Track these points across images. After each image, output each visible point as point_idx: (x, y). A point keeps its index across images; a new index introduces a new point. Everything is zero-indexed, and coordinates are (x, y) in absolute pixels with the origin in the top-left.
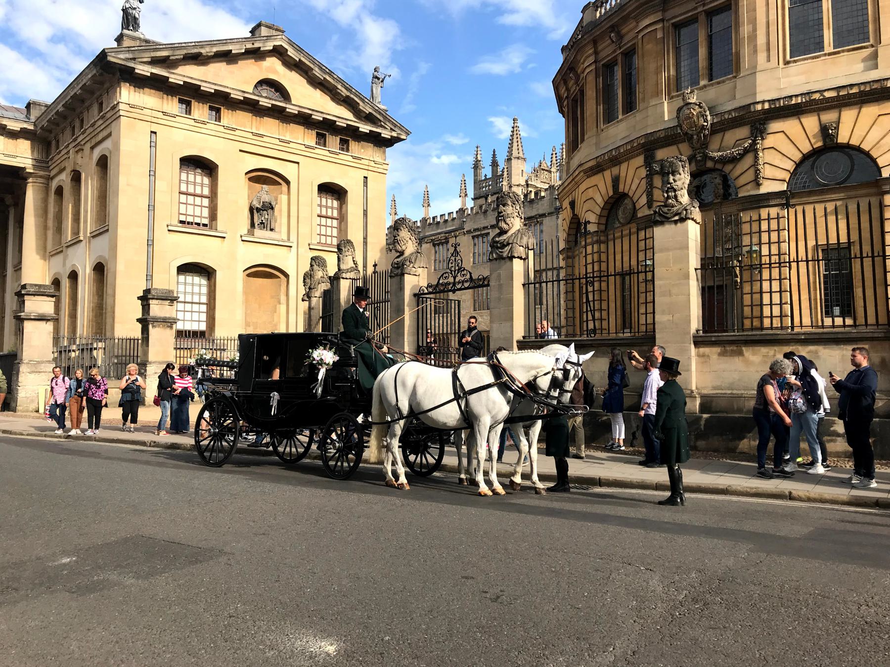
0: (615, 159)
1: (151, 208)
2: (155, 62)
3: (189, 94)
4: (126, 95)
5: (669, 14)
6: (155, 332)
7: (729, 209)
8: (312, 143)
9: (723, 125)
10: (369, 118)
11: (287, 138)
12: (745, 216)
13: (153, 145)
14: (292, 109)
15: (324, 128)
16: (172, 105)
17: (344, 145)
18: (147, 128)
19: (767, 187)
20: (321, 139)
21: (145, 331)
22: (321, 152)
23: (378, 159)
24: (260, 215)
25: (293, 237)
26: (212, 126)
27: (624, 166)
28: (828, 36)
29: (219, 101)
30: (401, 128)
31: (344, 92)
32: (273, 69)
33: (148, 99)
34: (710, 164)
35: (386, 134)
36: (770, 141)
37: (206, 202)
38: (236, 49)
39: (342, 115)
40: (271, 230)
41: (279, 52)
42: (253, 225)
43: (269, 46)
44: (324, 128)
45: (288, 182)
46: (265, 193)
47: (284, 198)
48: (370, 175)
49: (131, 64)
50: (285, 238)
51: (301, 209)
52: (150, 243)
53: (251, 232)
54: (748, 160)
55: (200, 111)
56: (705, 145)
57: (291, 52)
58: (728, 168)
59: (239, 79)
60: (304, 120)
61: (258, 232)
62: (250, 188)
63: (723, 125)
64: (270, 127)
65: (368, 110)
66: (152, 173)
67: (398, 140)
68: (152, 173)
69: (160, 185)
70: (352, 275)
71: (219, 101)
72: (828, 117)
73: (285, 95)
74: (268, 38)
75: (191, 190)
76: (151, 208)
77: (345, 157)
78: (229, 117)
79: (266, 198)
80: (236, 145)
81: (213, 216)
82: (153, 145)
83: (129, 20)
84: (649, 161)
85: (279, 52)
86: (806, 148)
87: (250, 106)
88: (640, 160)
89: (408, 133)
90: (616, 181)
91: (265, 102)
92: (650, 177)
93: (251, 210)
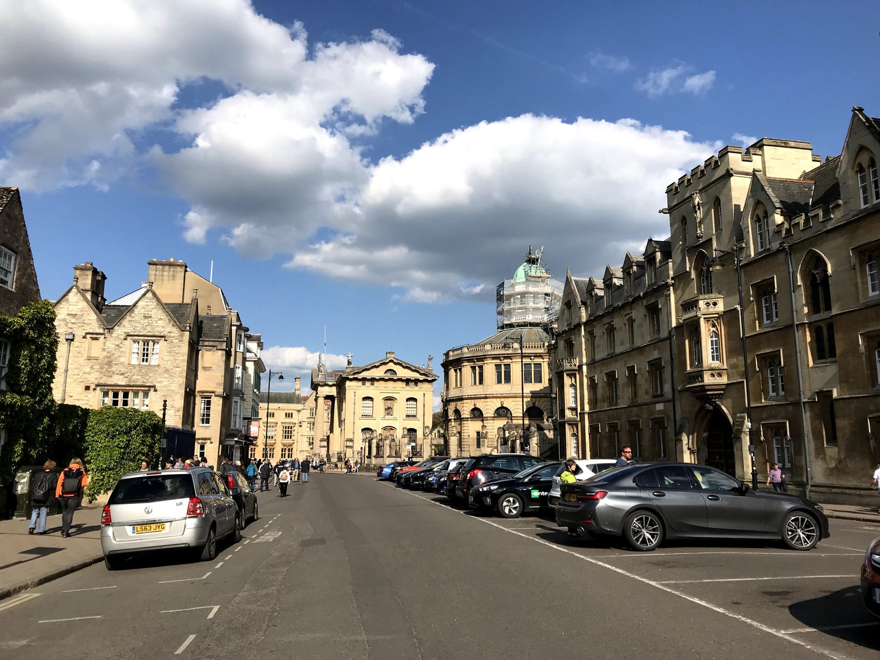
2: (354, 374)
3: (364, 380)
4: (348, 383)
10: (424, 374)
15: (408, 381)
16: (360, 383)
22: (408, 388)
24: (389, 409)
26: (372, 387)
29: (373, 380)
32: (391, 366)
33: (354, 383)
35: (430, 379)
41: (391, 361)
44: (408, 381)
46: (389, 403)
51: (401, 407)
55: (368, 384)
60: (400, 380)
64: (390, 383)
73: (393, 372)
77: (416, 388)
78: (376, 383)
80: (378, 391)
85: (391, 361)
87: (382, 379)
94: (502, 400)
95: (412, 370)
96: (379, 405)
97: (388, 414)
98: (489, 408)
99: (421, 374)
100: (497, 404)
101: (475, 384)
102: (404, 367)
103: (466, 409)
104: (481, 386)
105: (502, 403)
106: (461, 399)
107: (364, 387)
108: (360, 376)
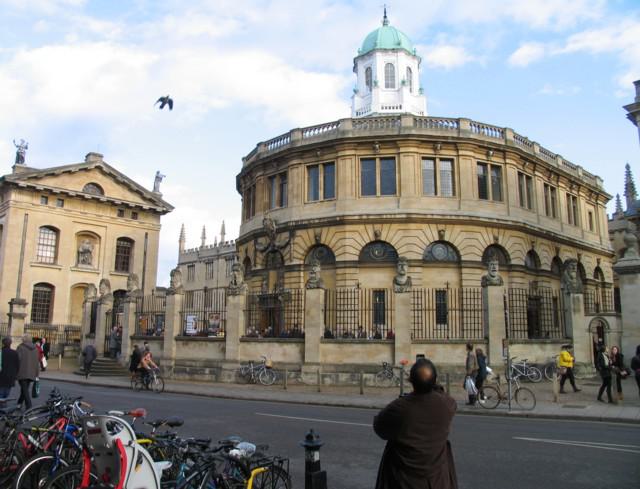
1: (22, 253)
4: (14, 196)
5: (268, 172)
6: (15, 321)
7: (281, 271)
8: (115, 216)
9: (281, 230)
10: (150, 200)
11: (101, 214)
12: (287, 275)
13: (26, 221)
14: (103, 199)
15: (122, 209)
16: (38, 201)
17: (135, 216)
18: (23, 212)
19: (296, 262)
20: (121, 214)
21: (10, 320)
22: (120, 220)
23: (155, 223)
24: (84, 256)
25: (101, 268)
26: (59, 209)
29: (64, 197)
30: (169, 205)
31: (136, 188)
33: (25, 199)
35: (159, 209)
36: (297, 240)
37: (53, 249)
38: (73, 169)
39: (133, 199)
40: (89, 264)
41: (99, 168)
42: (78, 261)
43: (93, 166)
45: (100, 238)
47: (97, 246)
48: (149, 232)
49: (17, 182)
50: (96, 267)
52: (20, 272)
53: (76, 266)
54: (288, 249)
57: (105, 169)
59: (75, 185)
60: (111, 203)
61: (80, 266)
62: (78, 241)
63: (281, 230)
65: (149, 197)
66: (24, 235)
67: (164, 213)
68: (24, 235)
69: (28, 242)
70: (92, 300)
71: (64, 197)
72: (318, 230)
73: (102, 192)
74: (93, 162)
75: (45, 243)
76: (22, 253)
77: (135, 223)
79: (87, 246)
81: (56, 258)
82: (26, 221)
83: (20, 158)
84: (256, 243)
86: (309, 245)
88: (252, 242)
89: (173, 208)
90: (246, 251)
91: (87, 196)
92: (256, 250)
93: (78, 252)
94: (441, 227)
95: (131, 190)
96: (69, 245)
97: (84, 262)
98: (411, 242)
99: (144, 198)
100: (431, 233)
102: (118, 182)
103: (350, 244)
104: (391, 198)
105: (441, 233)
106: (339, 222)
107: (44, 208)
108: (42, 184)
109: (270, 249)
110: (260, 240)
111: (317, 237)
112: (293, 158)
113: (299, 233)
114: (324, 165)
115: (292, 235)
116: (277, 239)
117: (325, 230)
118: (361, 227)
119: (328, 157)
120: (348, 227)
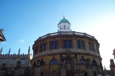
0: (54, 54)
5: (63, 39)
27: (56, 56)
28: (81, 47)
34: (70, 58)
36: (77, 57)
54: (75, 59)
56: (69, 55)
58: (72, 59)
72: (83, 56)
84: (61, 56)
90: (54, 58)
101: (91, 50)
106: (88, 54)
109: (67, 58)
110: (63, 55)
111: (83, 57)
112: (74, 37)
113: (78, 55)
114: (81, 41)
115: (76, 56)
116: (70, 56)
117: (84, 56)
118: (91, 57)
119: (83, 40)
120: (89, 56)
